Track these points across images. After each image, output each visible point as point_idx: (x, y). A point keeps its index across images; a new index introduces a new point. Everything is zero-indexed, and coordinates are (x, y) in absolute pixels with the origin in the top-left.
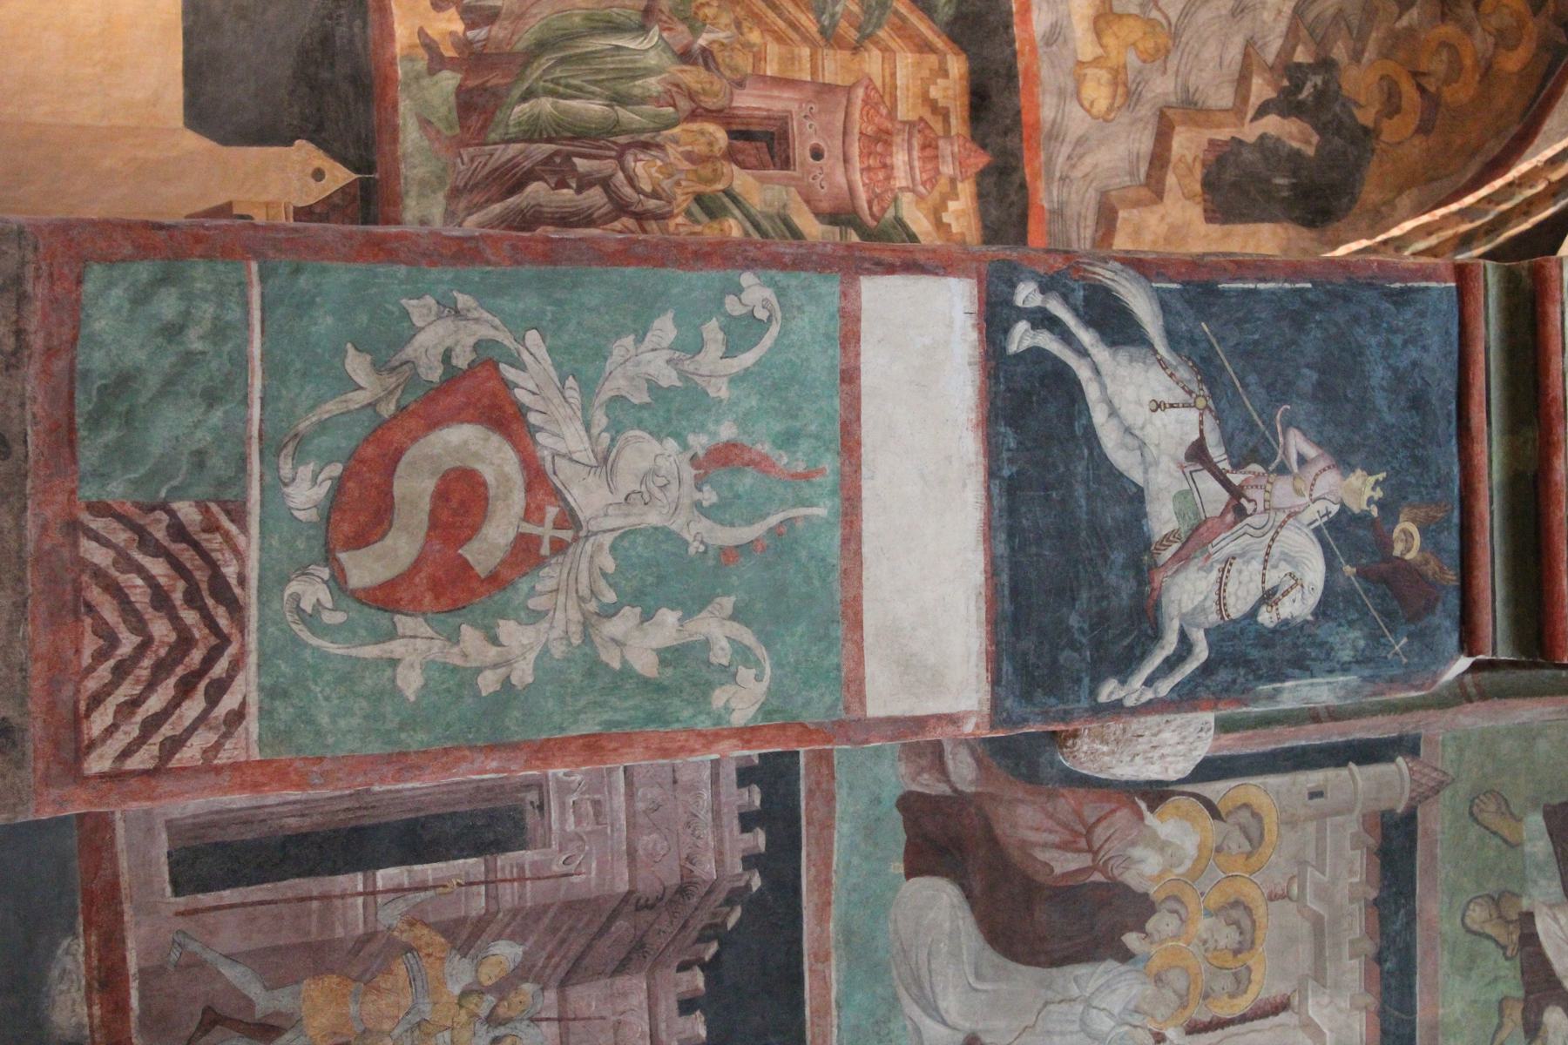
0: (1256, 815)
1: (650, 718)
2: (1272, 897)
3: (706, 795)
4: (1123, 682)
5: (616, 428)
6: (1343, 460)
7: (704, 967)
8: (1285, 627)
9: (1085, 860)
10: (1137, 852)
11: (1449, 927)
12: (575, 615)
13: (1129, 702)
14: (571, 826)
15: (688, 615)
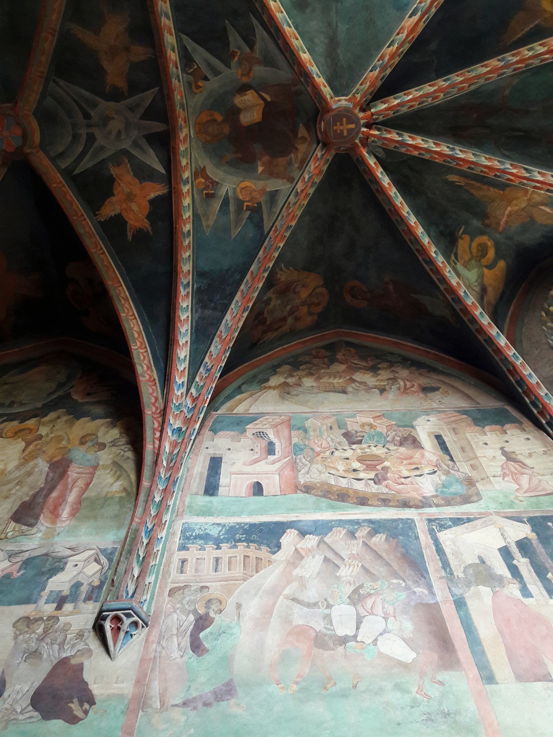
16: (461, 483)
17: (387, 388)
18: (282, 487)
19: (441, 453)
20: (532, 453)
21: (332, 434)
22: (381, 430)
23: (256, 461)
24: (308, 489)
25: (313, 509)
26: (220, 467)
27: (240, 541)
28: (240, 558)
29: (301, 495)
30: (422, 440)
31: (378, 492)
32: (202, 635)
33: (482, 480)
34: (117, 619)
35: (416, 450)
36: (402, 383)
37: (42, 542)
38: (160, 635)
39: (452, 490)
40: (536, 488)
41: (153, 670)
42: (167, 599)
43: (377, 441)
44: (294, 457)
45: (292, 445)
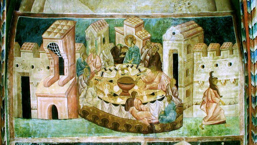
16: (175, 110)
18: (69, 111)
19: (171, 76)
20: (227, 80)
22: (138, 46)
23: (52, 82)
25: (87, 133)
29: (80, 120)
30: (164, 60)
31: (126, 118)
33: (188, 107)
35: (157, 72)
39: (168, 118)
40: (216, 117)
44: (77, 78)
45: (76, 62)
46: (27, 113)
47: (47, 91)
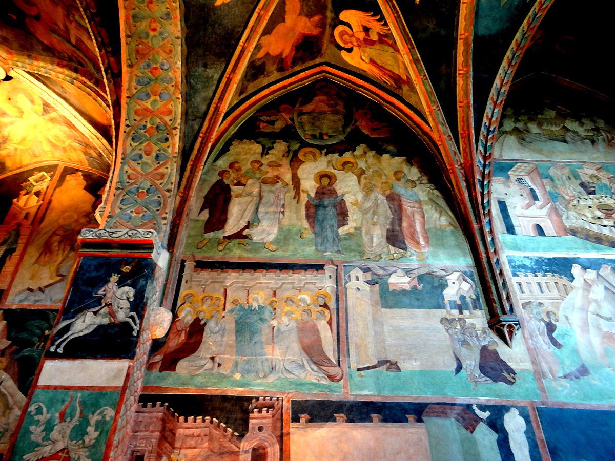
0: (187, 295)
1: (107, 434)
2: (204, 292)
3: (146, 414)
4: (134, 330)
5: (48, 439)
6: (107, 282)
7: (179, 416)
8: (135, 296)
9: (184, 332)
10: (186, 321)
11: (221, 254)
12: (81, 450)
13: (138, 329)
14: (143, 445)
15: (89, 425)
17: (595, 138)
21: (572, 183)
23: (528, 206)
24: (574, 232)
26: (507, 210)
27: (546, 271)
28: (552, 284)
29: (570, 237)
32: (554, 335)
34: (510, 326)
36: (604, 135)
37: (421, 263)
38: (530, 334)
41: (537, 356)
42: (523, 311)
43: (606, 193)
46: (510, 229)
47: (526, 212)
